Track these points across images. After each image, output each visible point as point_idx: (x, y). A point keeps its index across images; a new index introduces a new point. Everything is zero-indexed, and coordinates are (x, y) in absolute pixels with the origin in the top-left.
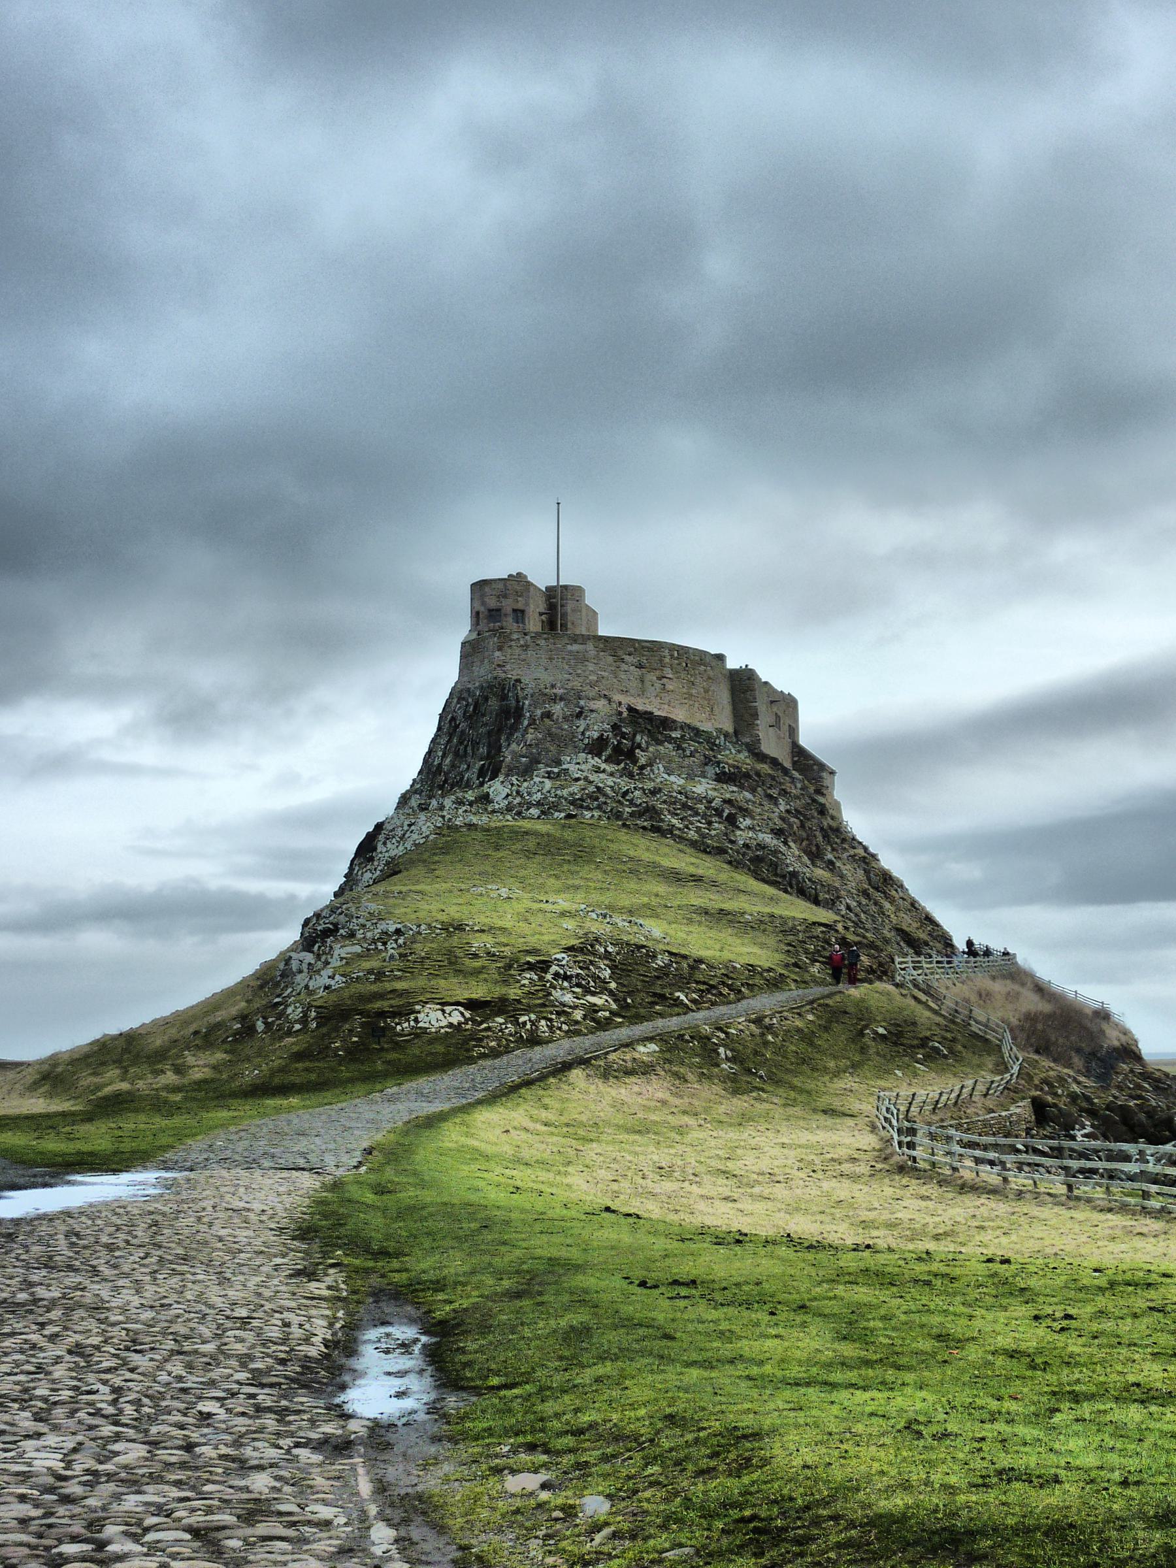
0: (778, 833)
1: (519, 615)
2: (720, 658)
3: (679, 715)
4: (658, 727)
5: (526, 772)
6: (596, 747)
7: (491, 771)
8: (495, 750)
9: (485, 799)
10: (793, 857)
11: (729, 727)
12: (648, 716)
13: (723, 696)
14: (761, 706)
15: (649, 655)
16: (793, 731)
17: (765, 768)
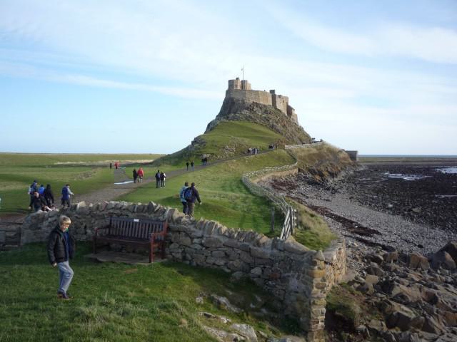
0: (277, 123)
1: (237, 86)
2: (272, 92)
3: (261, 103)
4: (257, 105)
5: (235, 113)
6: (247, 109)
7: (229, 113)
8: (230, 109)
9: (228, 117)
10: (279, 126)
11: (271, 104)
12: (257, 103)
13: (270, 99)
14: (278, 100)
15: (257, 93)
16: (287, 103)
17: (276, 111)
